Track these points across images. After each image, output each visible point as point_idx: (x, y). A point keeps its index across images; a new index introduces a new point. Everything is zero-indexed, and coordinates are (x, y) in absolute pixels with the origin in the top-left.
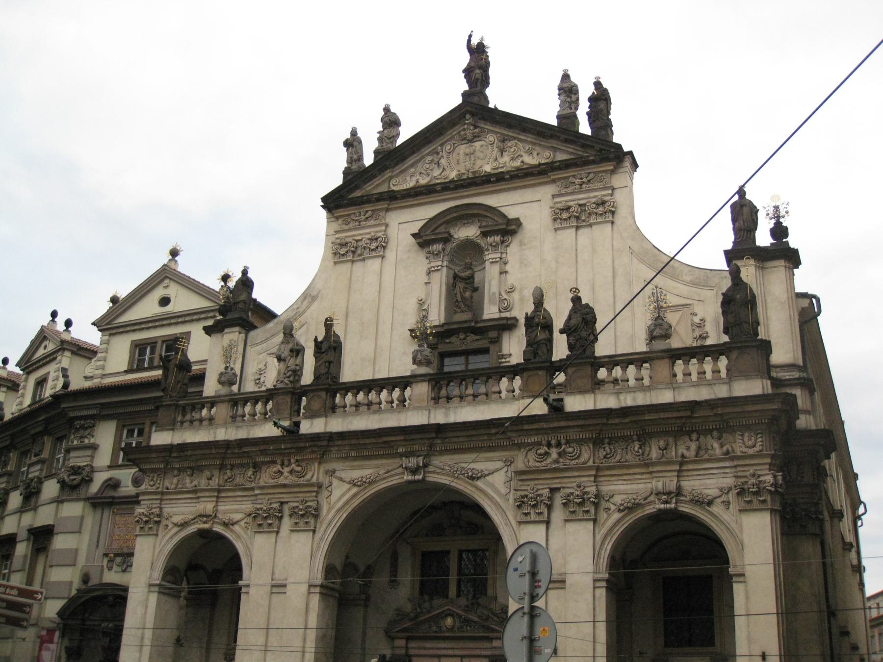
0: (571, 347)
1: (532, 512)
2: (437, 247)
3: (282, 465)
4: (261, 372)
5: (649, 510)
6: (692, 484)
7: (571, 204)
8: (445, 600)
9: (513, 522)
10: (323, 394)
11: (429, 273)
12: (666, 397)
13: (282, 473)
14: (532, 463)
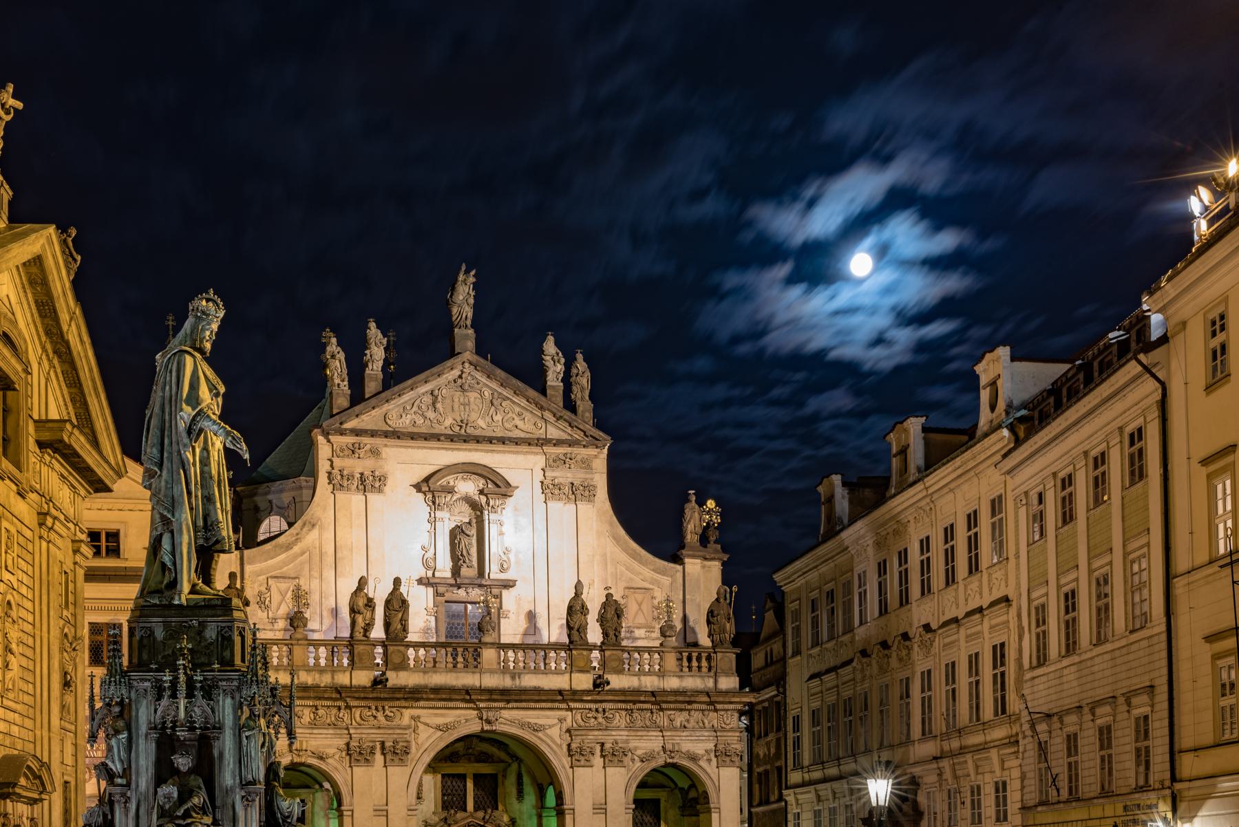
0: (605, 634)
1: (582, 759)
2: (443, 499)
3: (377, 709)
4: (260, 594)
5: (661, 762)
6: (687, 746)
7: (561, 480)
8: (460, 815)
9: (567, 766)
10: (402, 648)
11: (433, 521)
12: (673, 683)
13: (375, 717)
14: (582, 724)
